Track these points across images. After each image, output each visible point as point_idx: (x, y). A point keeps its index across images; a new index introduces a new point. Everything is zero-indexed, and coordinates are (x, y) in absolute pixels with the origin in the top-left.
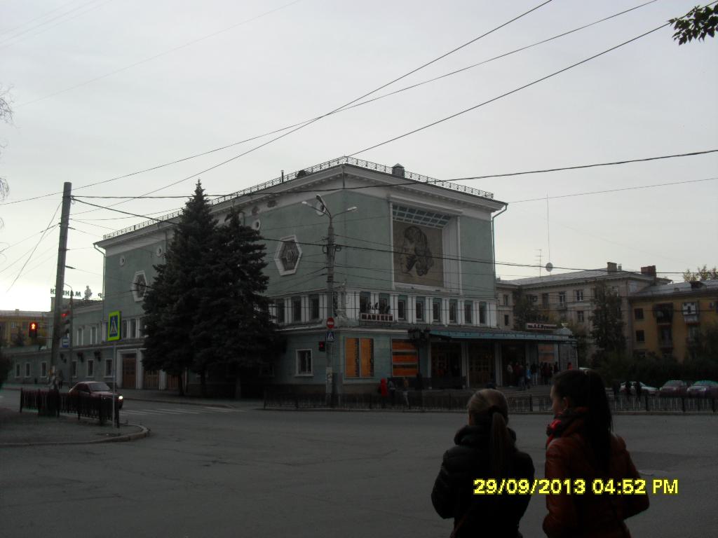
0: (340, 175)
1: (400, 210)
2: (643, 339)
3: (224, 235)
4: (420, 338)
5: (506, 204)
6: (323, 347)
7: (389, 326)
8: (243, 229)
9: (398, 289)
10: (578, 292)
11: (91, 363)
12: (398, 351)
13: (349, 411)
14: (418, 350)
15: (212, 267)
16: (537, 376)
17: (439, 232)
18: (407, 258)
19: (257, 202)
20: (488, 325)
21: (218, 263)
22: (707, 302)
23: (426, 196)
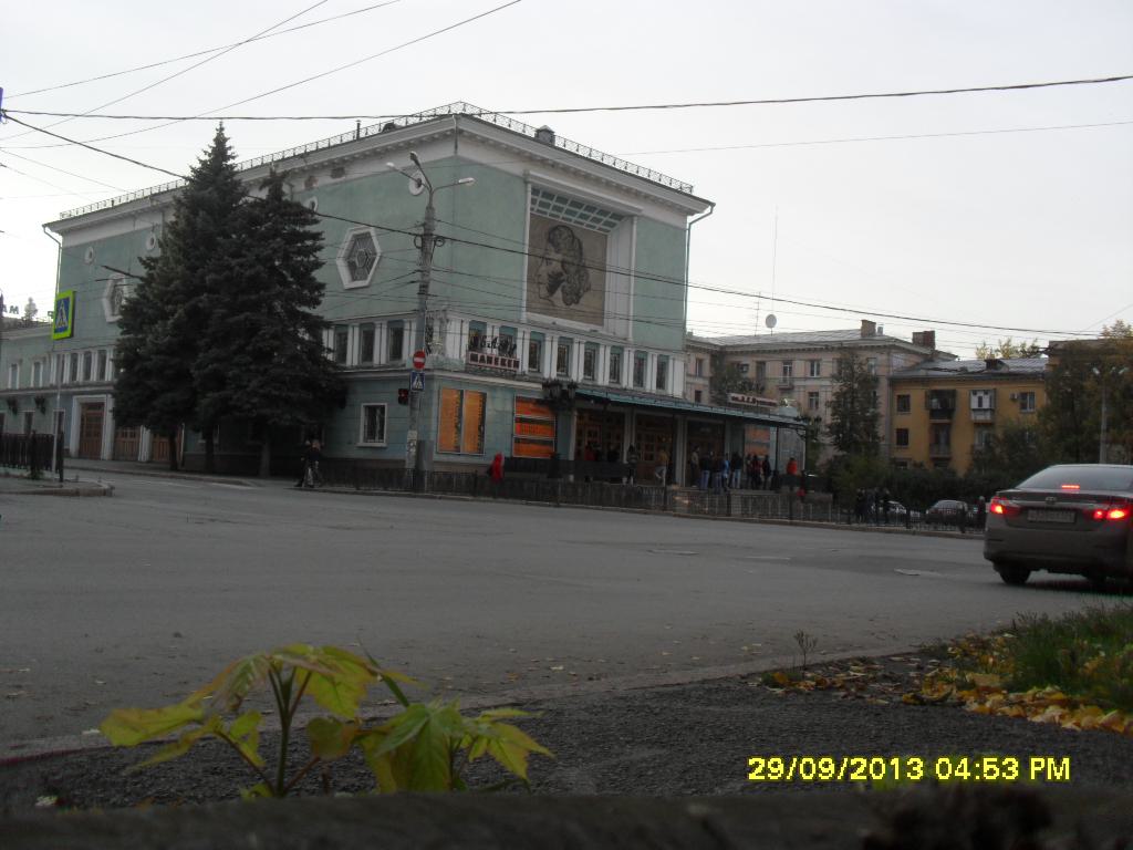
0: (452, 130)
2: (906, 443)
3: (257, 212)
4: (559, 398)
5: (713, 205)
6: (405, 397)
7: (513, 377)
8: (288, 204)
9: (531, 323)
10: (812, 362)
11: (29, 416)
12: (524, 416)
13: (440, 498)
14: (557, 416)
15: (234, 262)
16: (739, 474)
17: (603, 239)
18: (549, 276)
19: (314, 169)
20: (670, 392)
21: (245, 256)
22: (1009, 391)
23: (587, 177)
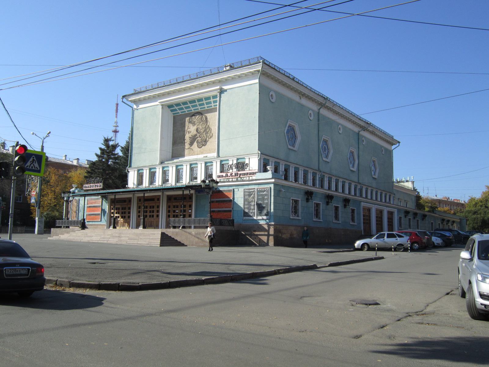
1: (198, 102)
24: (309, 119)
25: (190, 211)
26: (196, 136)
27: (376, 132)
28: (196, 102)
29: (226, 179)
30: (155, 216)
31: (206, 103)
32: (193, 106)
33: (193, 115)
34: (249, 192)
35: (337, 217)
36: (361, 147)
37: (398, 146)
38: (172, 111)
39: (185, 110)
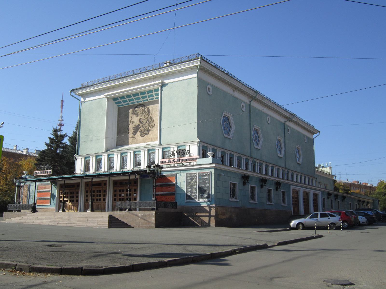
1: (141, 95)
24: (242, 110)
25: (135, 195)
26: (139, 126)
27: (299, 123)
28: (139, 95)
29: (169, 165)
30: (102, 200)
31: (148, 96)
32: (136, 99)
33: (136, 107)
34: (191, 176)
35: (270, 199)
36: (287, 136)
37: (318, 135)
38: (116, 103)
39: (129, 102)
